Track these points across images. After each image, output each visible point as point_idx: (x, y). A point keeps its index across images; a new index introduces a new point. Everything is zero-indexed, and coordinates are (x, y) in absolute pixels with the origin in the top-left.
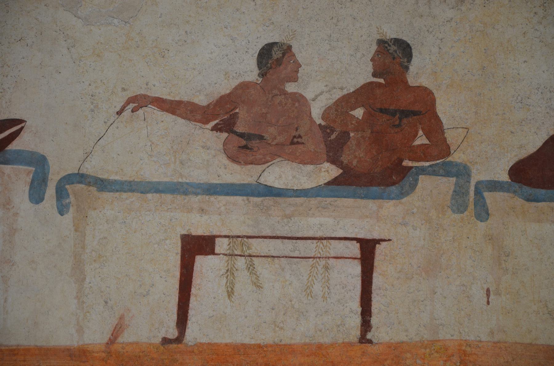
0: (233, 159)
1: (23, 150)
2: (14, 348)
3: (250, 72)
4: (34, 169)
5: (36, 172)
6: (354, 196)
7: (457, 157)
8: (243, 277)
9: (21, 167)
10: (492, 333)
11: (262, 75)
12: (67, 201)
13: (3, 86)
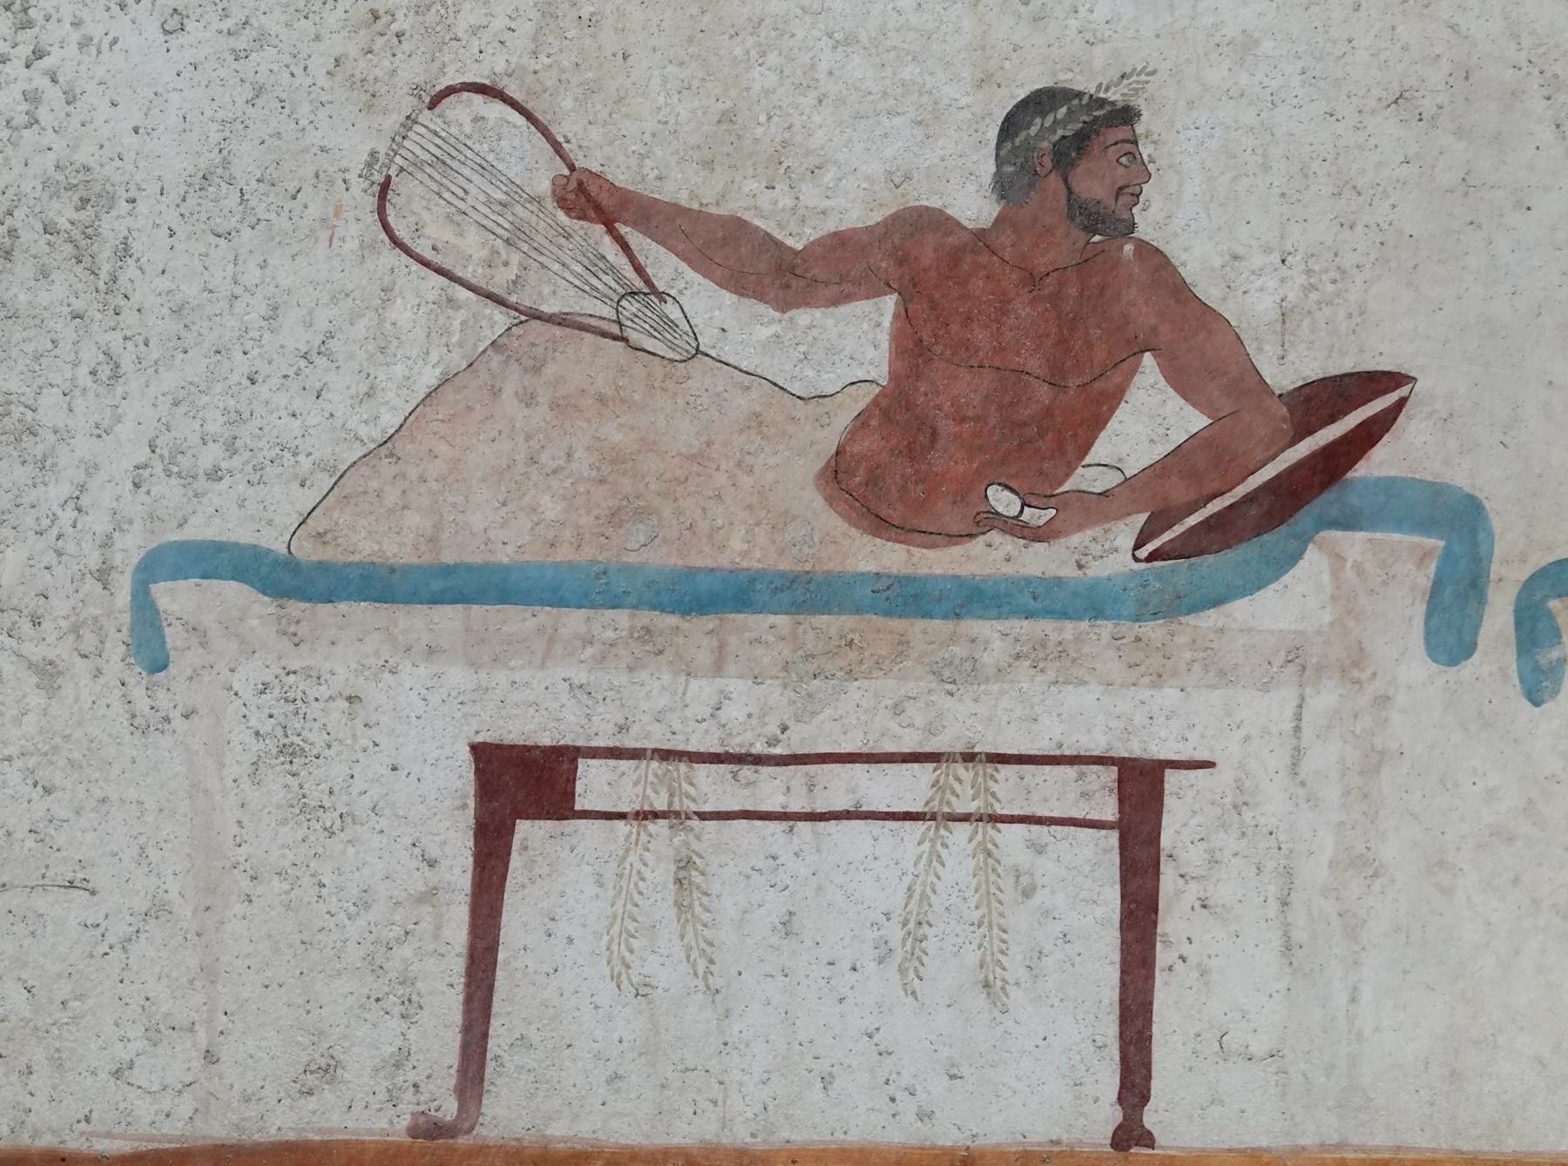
1: (1405, 480)
2: (1387, 1156)
4: (1442, 543)
5: (1447, 556)
9: (1397, 536)
12: (1555, 654)
13: (1338, 259)
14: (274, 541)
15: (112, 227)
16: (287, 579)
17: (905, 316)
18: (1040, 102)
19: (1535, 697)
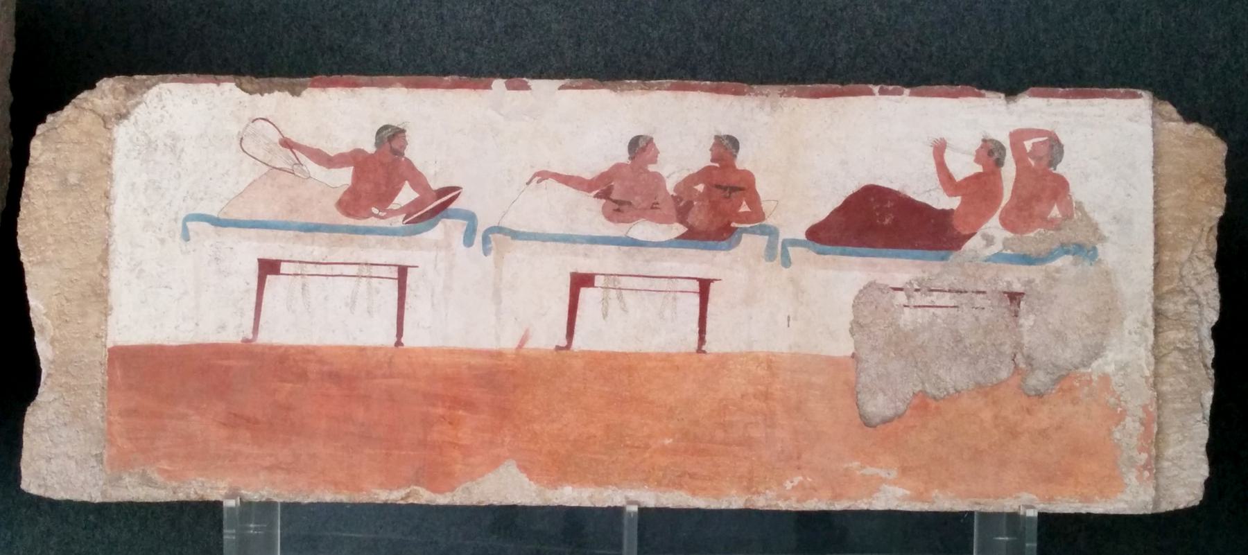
0: (609, 218)
3: (623, 156)
6: (696, 247)
7: (770, 221)
8: (614, 304)
10: (790, 347)
11: (632, 158)
14: (215, 214)
15: (179, 145)
16: (217, 222)
17: (355, 172)
18: (385, 127)
19: (486, 255)
